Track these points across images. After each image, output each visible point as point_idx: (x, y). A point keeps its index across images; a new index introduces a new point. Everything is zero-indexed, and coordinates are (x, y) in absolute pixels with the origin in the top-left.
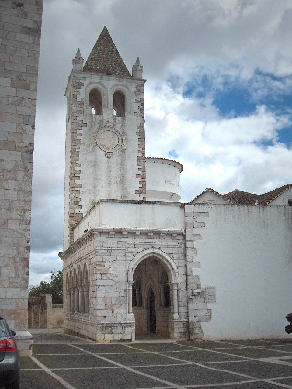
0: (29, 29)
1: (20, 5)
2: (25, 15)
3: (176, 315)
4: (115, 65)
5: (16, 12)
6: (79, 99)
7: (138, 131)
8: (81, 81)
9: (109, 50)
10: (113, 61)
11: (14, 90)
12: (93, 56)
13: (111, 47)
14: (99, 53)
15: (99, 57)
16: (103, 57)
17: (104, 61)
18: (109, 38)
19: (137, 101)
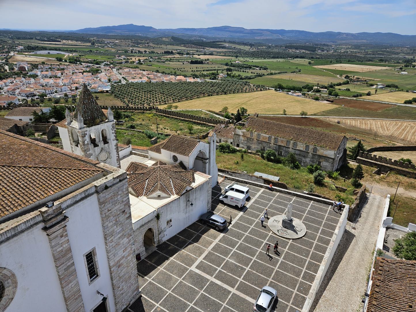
0: (128, 217)
1: (125, 211)
2: (126, 213)
3: (155, 240)
4: (97, 112)
5: (123, 215)
6: (86, 143)
7: (115, 147)
8: (85, 133)
9: (91, 102)
10: (96, 109)
11: (128, 239)
12: (84, 110)
13: (92, 99)
14: (87, 106)
15: (88, 109)
16: (90, 108)
17: (91, 111)
18: (89, 92)
19: (113, 133)
